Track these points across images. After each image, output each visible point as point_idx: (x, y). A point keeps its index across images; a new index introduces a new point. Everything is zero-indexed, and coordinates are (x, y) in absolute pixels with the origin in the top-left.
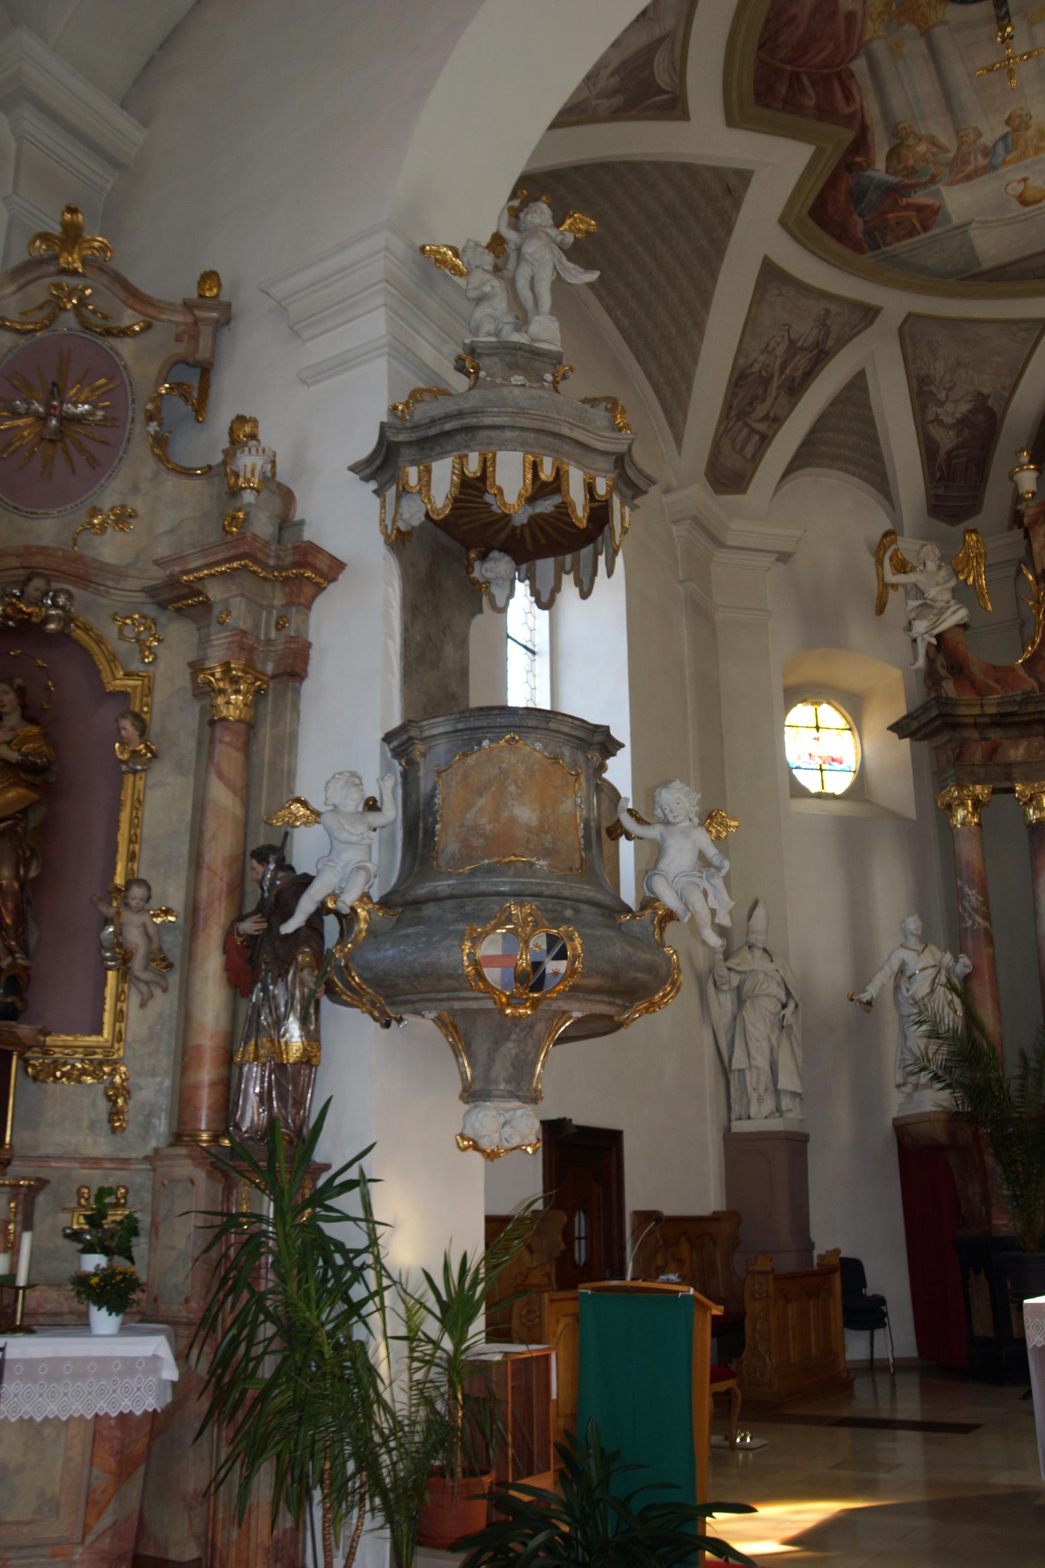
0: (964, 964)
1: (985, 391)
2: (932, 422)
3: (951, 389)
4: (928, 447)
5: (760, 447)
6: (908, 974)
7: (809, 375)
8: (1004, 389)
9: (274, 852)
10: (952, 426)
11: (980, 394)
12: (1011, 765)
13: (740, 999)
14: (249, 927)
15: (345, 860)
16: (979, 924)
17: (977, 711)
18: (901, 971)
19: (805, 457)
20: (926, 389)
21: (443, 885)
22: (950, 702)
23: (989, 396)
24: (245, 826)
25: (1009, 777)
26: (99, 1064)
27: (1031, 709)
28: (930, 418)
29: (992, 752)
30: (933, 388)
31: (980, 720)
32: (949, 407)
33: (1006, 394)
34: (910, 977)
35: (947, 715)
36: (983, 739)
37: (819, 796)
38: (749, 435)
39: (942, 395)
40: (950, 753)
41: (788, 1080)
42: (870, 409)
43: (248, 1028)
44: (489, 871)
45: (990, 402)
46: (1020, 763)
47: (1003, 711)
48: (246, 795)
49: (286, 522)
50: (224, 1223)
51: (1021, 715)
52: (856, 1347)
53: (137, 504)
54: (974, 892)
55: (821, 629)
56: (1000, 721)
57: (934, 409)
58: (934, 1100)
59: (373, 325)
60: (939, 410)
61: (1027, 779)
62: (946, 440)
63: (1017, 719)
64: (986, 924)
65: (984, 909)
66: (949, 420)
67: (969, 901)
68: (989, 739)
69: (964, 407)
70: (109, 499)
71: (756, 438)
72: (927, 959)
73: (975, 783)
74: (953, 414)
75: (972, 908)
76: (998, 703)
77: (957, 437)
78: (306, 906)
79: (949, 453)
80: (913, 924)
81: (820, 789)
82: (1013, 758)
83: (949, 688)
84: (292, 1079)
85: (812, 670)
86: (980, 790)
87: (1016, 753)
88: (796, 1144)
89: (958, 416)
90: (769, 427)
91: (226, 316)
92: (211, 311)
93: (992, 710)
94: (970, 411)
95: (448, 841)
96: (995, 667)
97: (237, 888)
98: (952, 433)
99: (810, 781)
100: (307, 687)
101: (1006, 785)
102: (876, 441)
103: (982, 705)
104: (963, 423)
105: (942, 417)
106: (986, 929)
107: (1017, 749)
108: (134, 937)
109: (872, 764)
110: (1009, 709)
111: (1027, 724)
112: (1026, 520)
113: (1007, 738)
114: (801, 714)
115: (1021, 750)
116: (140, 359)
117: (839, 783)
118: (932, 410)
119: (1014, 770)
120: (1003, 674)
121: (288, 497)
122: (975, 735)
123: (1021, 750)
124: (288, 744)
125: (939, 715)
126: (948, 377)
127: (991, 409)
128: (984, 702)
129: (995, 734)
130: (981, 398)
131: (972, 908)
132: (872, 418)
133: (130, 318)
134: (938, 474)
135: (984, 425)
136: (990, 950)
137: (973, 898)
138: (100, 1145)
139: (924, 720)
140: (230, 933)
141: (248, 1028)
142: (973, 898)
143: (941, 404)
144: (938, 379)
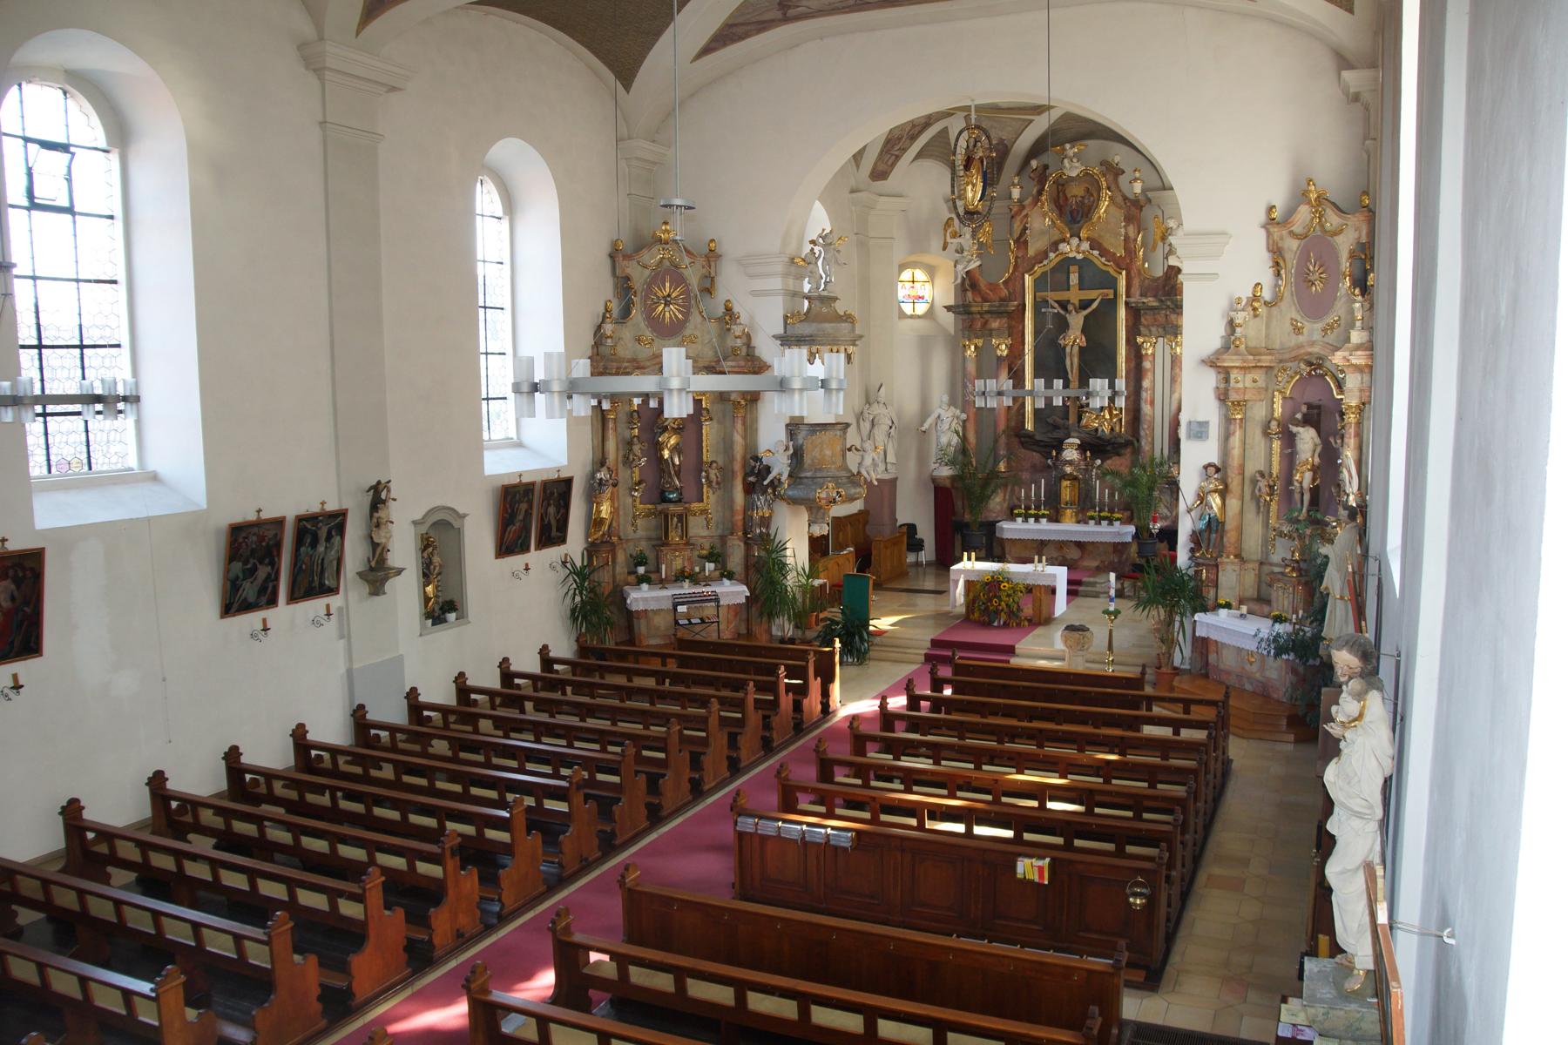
0: (964, 416)
7: (920, 132)
9: (757, 459)
13: (873, 424)
14: (751, 479)
15: (780, 466)
19: (919, 156)
21: (809, 474)
22: (969, 305)
24: (746, 447)
26: (704, 512)
29: (986, 323)
37: (912, 317)
41: (891, 458)
43: (749, 506)
44: (820, 470)
48: (745, 438)
49: (749, 345)
50: (748, 555)
52: (911, 558)
53: (697, 333)
55: (917, 243)
58: (946, 472)
59: (776, 283)
61: (998, 337)
70: (687, 332)
72: (950, 414)
78: (770, 477)
80: (946, 398)
83: (969, 294)
84: (766, 522)
85: (913, 258)
86: (980, 342)
87: (995, 324)
88: (893, 482)
91: (719, 256)
92: (712, 256)
95: (807, 460)
97: (744, 465)
99: (907, 309)
100: (760, 404)
108: (713, 477)
114: (906, 275)
116: (693, 276)
117: (921, 309)
120: (993, 287)
121: (749, 336)
124: (755, 421)
130: (1001, 141)
133: (687, 260)
135: (1004, 150)
138: (705, 533)
140: (744, 480)
141: (749, 506)
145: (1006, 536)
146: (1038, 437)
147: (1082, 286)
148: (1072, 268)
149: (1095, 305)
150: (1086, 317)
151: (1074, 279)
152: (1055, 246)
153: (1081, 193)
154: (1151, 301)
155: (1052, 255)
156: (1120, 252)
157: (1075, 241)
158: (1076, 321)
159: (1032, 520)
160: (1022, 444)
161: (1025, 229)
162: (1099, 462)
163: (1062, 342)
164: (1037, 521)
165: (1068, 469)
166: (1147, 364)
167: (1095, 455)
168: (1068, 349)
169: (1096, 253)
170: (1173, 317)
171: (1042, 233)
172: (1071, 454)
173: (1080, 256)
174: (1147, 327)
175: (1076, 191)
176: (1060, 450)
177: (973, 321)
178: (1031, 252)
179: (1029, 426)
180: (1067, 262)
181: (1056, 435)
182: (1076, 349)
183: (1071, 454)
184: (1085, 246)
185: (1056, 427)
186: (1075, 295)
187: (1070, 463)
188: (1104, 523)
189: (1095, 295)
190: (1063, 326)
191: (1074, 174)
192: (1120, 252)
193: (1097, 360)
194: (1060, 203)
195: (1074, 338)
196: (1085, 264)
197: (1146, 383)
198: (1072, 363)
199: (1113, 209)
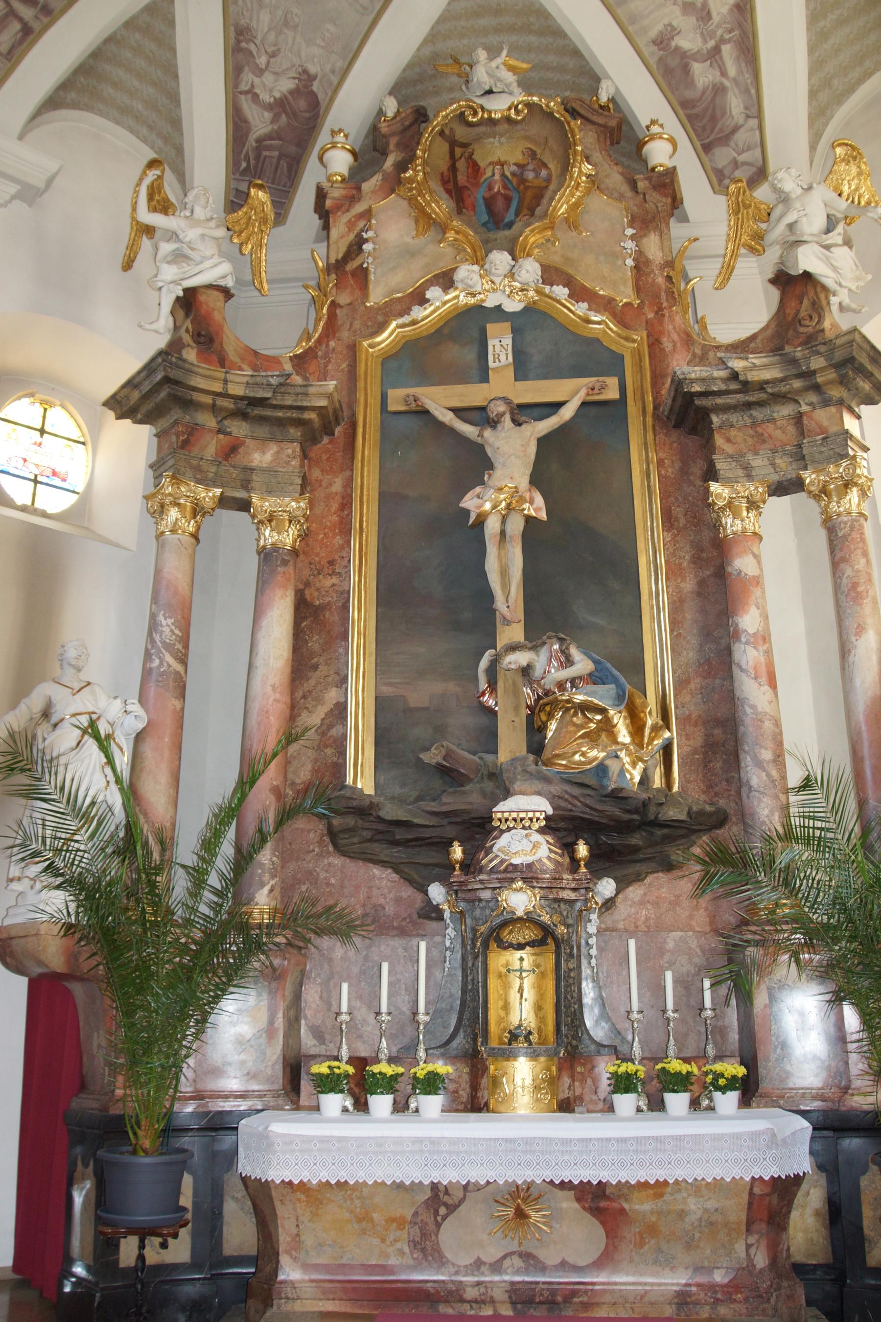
1: (313, 69)
2: (246, 93)
3: (273, 55)
4: (238, 127)
5: (21, 42)
6: (54, 719)
8: (333, 72)
10: (269, 107)
11: (305, 71)
12: (252, 470)
16: (169, 666)
17: (217, 387)
18: (46, 714)
20: (243, 45)
23: (315, 78)
25: (246, 485)
27: (288, 402)
28: (244, 87)
29: (231, 450)
30: (252, 47)
31: (220, 402)
32: (268, 78)
33: (335, 80)
34: (55, 726)
35: (177, 383)
36: (219, 431)
38: (6, 16)
39: (262, 60)
40: (174, 438)
42: (173, 51)
45: (315, 87)
46: (263, 470)
47: (252, 394)
51: (275, 407)
54: (170, 621)
56: (249, 408)
57: (251, 76)
60: (257, 81)
62: (261, 123)
63: (268, 412)
64: (179, 667)
65: (179, 646)
66: (265, 97)
67: (162, 632)
68: (230, 434)
69: (286, 85)
71: (16, 26)
73: (199, 481)
74: (271, 90)
75: (163, 642)
76: (247, 383)
77: (272, 122)
79: (259, 141)
81: (29, 503)
82: (255, 464)
86: (209, 495)
87: (262, 457)
89: (278, 95)
90: (36, 17)
93: (237, 390)
94: (291, 92)
96: (256, 353)
98: (268, 115)
101: (241, 494)
102: (174, 98)
103: (226, 381)
104: (280, 106)
105: (257, 91)
106: (177, 673)
107: (264, 453)
109: (100, 483)
110: (261, 394)
111: (281, 423)
112: (328, 203)
113: (253, 438)
115: (268, 457)
118: (248, 78)
119: (254, 477)
122: (209, 421)
123: (268, 457)
125: (167, 380)
126: (272, 37)
127: (314, 95)
128: (230, 377)
129: (239, 428)
130: (306, 78)
131: (163, 642)
132: (175, 66)
134: (244, 165)
135: (303, 114)
136: (178, 704)
137: (167, 630)
139: (146, 387)
142: (167, 630)
143: (260, 72)
144: (260, 37)
145: (277, 1171)
146: (390, 812)
147: (522, 368)
148: (491, 328)
149: (567, 413)
150: (543, 442)
151: (500, 346)
152: (446, 280)
153: (518, 156)
154: (760, 368)
155: (433, 293)
156: (626, 295)
157: (500, 259)
158: (513, 451)
159: (381, 1103)
160: (333, 834)
161: (360, 242)
162: (607, 887)
163: (469, 502)
164: (400, 1107)
165: (519, 900)
166: (743, 564)
167: (606, 860)
168: (492, 525)
169: (561, 292)
170: (823, 416)
171: (411, 253)
172: (522, 844)
173: (513, 306)
174: (737, 458)
175: (500, 154)
176: (480, 829)
177: (194, 430)
178: (376, 296)
179: (362, 776)
180: (472, 322)
181: (451, 802)
182: (516, 526)
183: (522, 844)
184: (530, 270)
185: (450, 775)
186: (502, 386)
187: (528, 875)
188: (677, 1102)
189: (571, 393)
190: (476, 465)
191: (498, 106)
192: (626, 295)
193: (577, 572)
194: (459, 182)
195: (506, 495)
196: (529, 322)
197: (748, 621)
198: (505, 569)
199: (599, 202)
